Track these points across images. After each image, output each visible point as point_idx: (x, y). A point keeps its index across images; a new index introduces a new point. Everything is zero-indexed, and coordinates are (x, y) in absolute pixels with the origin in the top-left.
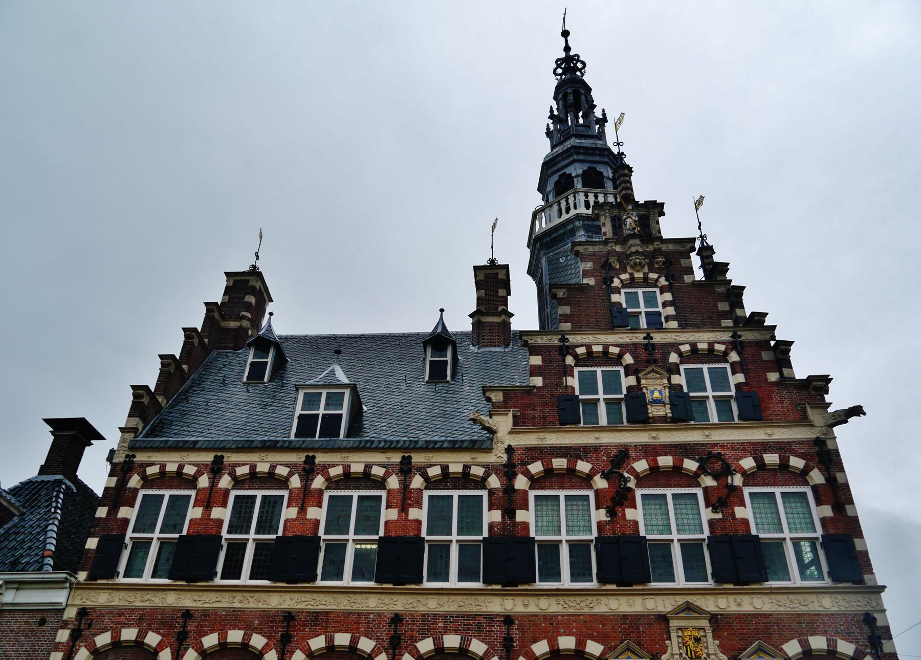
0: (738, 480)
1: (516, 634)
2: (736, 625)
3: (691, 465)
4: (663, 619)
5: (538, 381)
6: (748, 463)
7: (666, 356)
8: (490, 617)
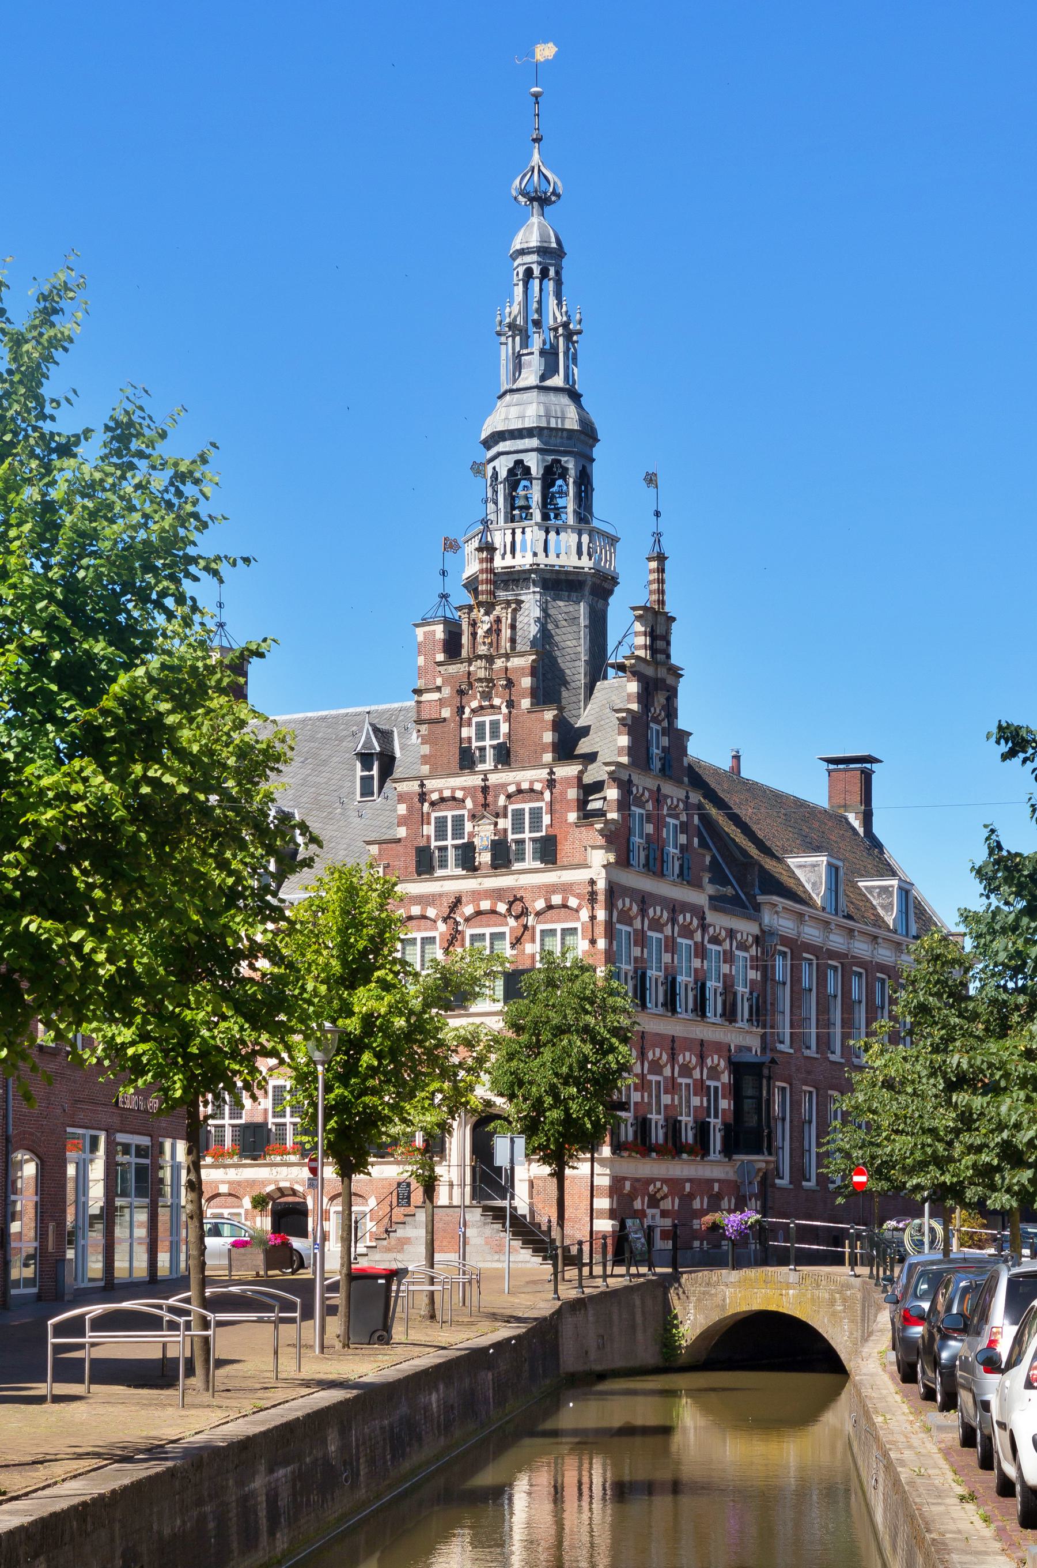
0: (531, 920)
3: (502, 908)
5: (402, 832)
6: (540, 904)
7: (496, 797)
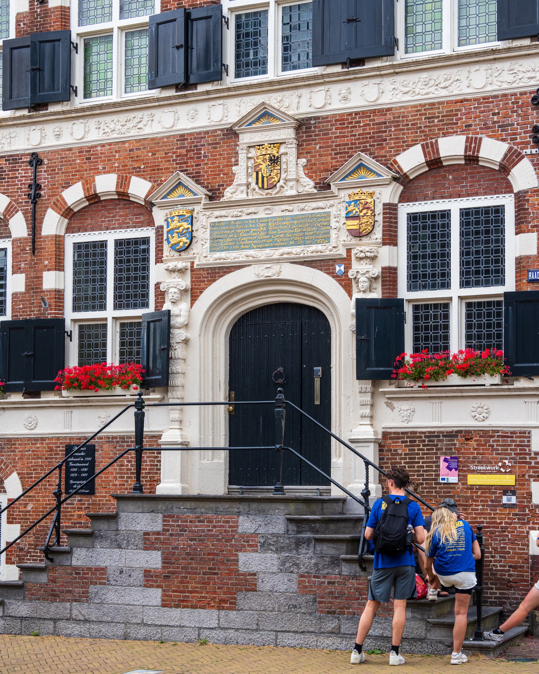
1: (44, 178)
2: (334, 132)
4: (231, 133)
8: (13, 159)
